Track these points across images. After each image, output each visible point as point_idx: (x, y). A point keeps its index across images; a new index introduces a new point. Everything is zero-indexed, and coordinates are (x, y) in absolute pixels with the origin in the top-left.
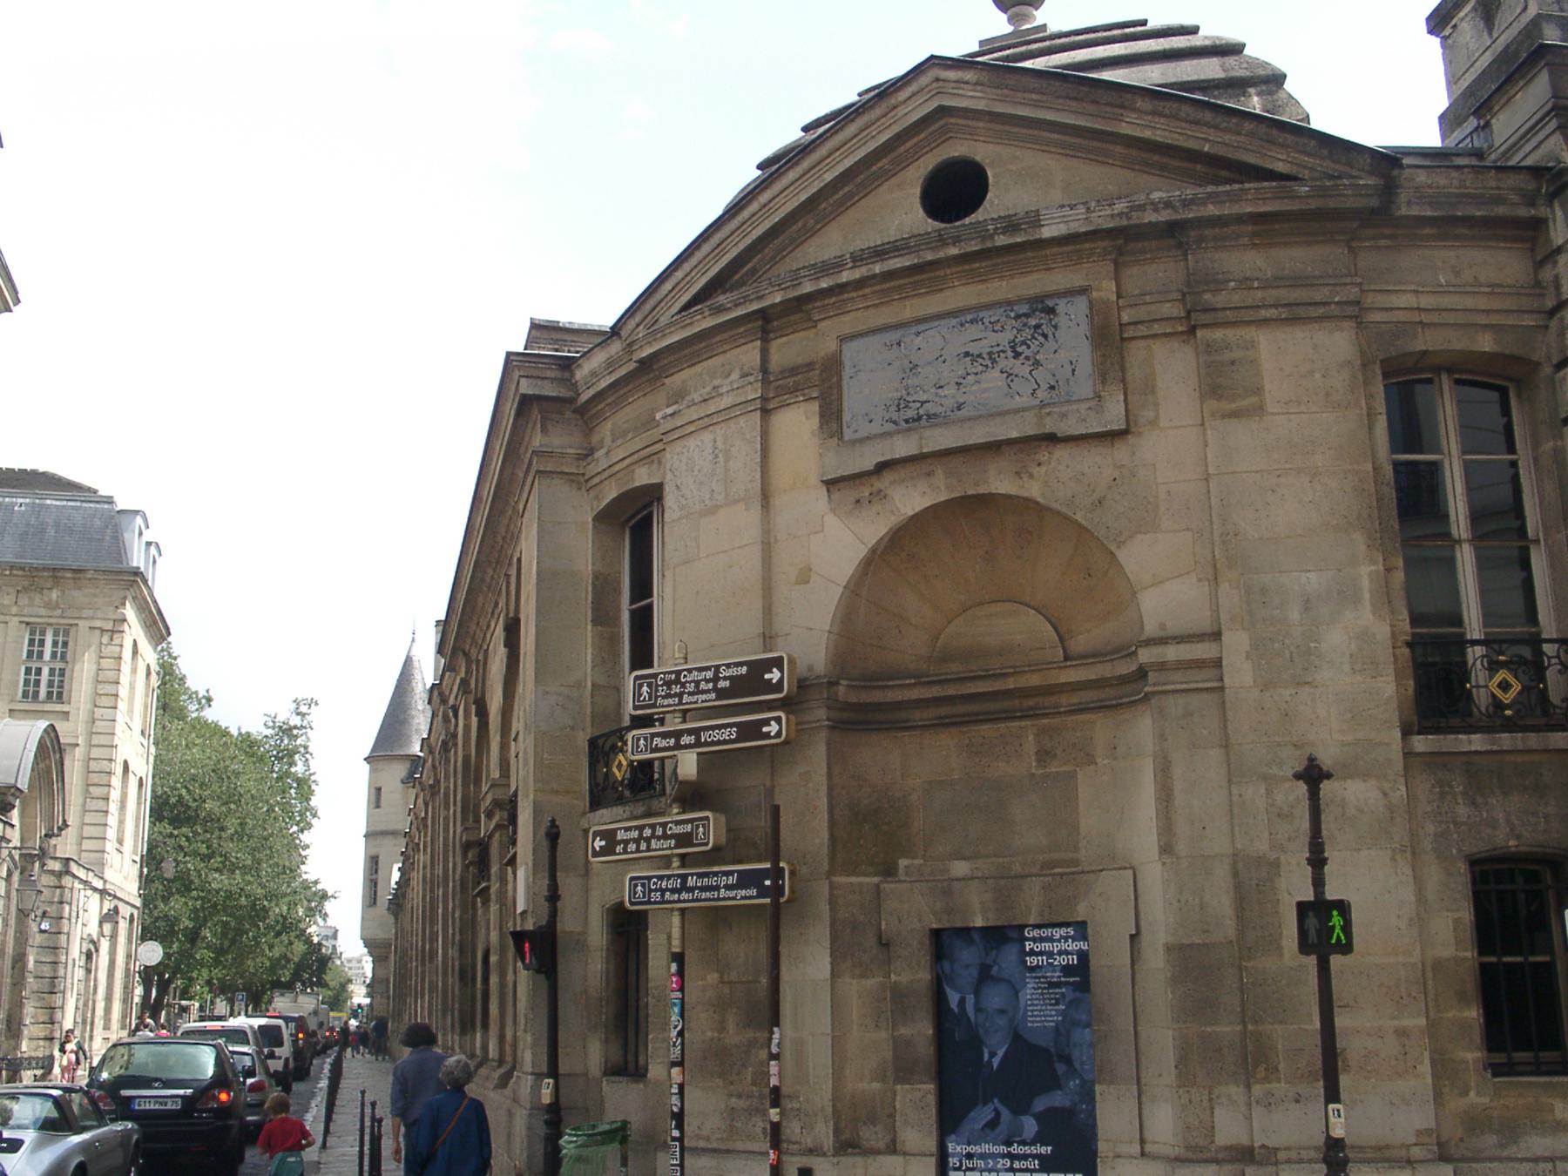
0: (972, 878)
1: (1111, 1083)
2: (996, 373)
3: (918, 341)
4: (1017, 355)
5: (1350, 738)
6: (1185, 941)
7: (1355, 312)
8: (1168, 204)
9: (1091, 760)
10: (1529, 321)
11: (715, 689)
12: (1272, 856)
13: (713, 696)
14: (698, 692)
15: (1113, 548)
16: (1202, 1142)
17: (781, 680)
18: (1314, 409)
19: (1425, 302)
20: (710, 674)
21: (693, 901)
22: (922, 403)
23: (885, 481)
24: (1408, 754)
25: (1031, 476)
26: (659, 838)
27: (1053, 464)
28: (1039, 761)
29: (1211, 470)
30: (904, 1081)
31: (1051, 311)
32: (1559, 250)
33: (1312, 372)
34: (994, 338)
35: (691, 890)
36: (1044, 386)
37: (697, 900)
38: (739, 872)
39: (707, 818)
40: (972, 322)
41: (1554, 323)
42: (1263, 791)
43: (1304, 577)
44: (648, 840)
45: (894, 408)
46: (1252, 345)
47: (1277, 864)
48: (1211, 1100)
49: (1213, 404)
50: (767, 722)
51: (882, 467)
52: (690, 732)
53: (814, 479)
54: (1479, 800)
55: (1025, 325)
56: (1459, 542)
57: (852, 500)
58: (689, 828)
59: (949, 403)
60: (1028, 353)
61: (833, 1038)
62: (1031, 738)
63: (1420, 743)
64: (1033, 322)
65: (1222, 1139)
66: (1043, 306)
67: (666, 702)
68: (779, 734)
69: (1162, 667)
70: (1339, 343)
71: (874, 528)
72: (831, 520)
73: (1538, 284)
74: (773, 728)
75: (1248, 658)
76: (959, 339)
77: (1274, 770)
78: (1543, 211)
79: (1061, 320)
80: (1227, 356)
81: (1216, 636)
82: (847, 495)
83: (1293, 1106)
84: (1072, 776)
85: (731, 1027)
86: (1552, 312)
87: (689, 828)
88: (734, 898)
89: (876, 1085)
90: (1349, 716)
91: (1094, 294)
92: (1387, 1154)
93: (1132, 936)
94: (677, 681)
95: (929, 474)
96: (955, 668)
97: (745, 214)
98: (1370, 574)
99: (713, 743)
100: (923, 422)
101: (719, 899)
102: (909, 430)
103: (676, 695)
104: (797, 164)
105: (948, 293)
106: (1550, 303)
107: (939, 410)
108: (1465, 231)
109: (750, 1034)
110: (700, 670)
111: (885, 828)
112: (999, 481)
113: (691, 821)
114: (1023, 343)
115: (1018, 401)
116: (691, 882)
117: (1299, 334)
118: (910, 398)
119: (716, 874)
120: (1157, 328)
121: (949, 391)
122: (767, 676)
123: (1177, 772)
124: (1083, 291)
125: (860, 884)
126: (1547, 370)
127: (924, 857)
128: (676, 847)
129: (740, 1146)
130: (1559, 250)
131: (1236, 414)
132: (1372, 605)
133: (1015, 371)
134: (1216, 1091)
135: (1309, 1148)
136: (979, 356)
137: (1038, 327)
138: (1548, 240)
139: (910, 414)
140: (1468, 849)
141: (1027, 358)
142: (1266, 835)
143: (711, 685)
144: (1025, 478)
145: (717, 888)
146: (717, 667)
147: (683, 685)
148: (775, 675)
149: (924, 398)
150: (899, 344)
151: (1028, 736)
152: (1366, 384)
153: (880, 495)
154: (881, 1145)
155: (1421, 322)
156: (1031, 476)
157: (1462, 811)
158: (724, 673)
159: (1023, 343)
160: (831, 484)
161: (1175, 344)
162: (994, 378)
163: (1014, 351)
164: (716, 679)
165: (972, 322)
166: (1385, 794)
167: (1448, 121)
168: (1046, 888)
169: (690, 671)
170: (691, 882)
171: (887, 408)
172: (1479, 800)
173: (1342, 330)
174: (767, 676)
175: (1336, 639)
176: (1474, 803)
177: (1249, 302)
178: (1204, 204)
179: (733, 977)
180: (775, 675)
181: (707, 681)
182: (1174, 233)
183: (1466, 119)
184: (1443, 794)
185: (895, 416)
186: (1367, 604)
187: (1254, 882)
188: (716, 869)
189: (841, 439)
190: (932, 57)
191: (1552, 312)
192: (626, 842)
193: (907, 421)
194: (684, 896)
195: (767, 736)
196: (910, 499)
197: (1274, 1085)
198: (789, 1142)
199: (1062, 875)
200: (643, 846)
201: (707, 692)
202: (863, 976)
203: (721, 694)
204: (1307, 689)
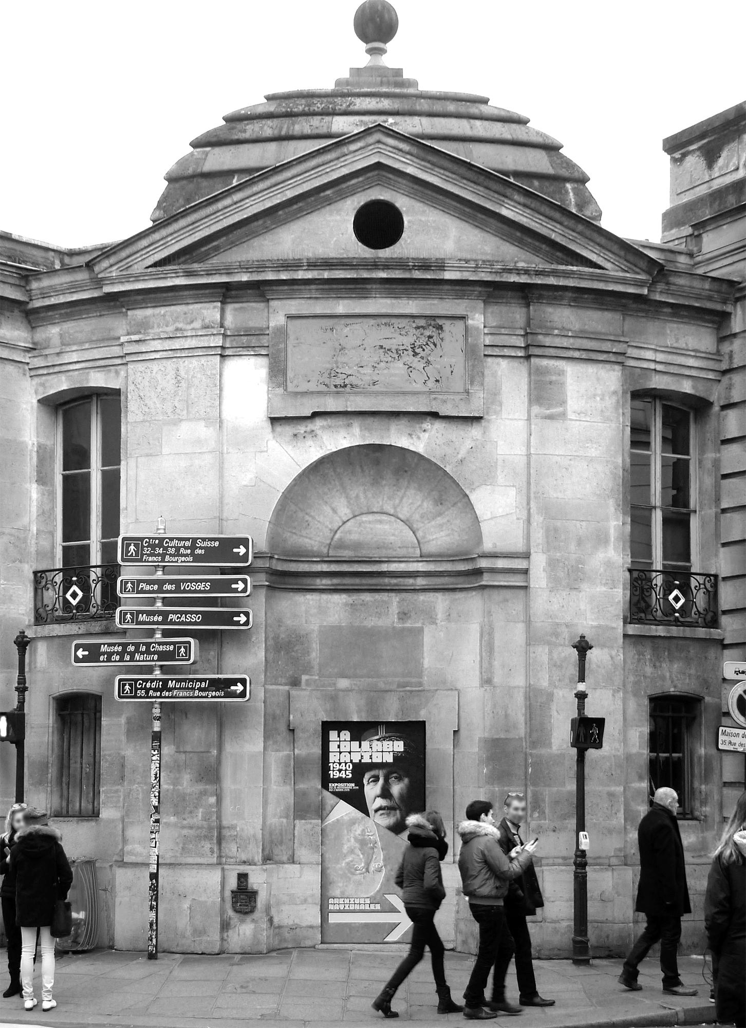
0: (351, 690)
2: (400, 364)
3: (346, 330)
4: (415, 354)
5: (595, 624)
7: (618, 359)
10: (711, 376)
11: (192, 554)
15: (467, 492)
20: (188, 544)
23: (319, 423)
24: (625, 636)
25: (419, 438)
26: (142, 653)
30: (302, 817)
31: (440, 328)
32: (735, 335)
36: (432, 379)
40: (386, 324)
41: (725, 380)
44: (132, 655)
45: (326, 375)
46: (562, 373)
49: (536, 409)
50: (236, 581)
51: (315, 415)
52: (171, 582)
54: (658, 664)
56: (655, 508)
57: (291, 434)
59: (367, 379)
60: (422, 354)
62: (395, 604)
63: (632, 629)
64: (427, 333)
66: (434, 321)
67: (150, 559)
68: (244, 590)
69: (493, 571)
70: (609, 379)
72: (273, 444)
73: (718, 352)
74: (241, 586)
76: (376, 335)
77: (554, 639)
78: (729, 308)
79: (446, 335)
80: (548, 378)
81: (527, 556)
82: (287, 430)
83: (552, 833)
84: (420, 631)
86: (724, 372)
87: (172, 648)
91: (470, 322)
92: (599, 861)
94: (160, 545)
96: (347, 554)
97: (220, 205)
99: (190, 591)
100: (348, 389)
102: (338, 393)
103: (159, 555)
104: (266, 178)
105: (370, 301)
106: (724, 366)
107: (360, 383)
108: (685, 313)
109: (200, 787)
110: (180, 539)
112: (398, 437)
113: (174, 643)
115: (419, 387)
116: (170, 684)
117: (591, 369)
119: (192, 680)
120: (506, 352)
121: (368, 370)
122: (235, 550)
123: (497, 636)
124: (463, 318)
126: (716, 408)
130: (735, 335)
131: (551, 417)
133: (414, 365)
137: (430, 337)
138: (729, 327)
139: (338, 382)
140: (649, 692)
141: (422, 358)
143: (189, 551)
144: (415, 439)
146: (194, 540)
147: (166, 549)
150: (332, 329)
151: (395, 599)
152: (623, 405)
154: (285, 858)
155: (655, 370)
156: (419, 438)
157: (649, 670)
158: (199, 544)
161: (515, 363)
162: (398, 367)
163: (414, 351)
164: (193, 547)
165: (386, 324)
166: (612, 658)
167: (671, 219)
168: (401, 699)
169: (171, 539)
170: (170, 684)
171: (322, 374)
172: (658, 664)
173: (614, 370)
174: (235, 550)
177: (565, 345)
178: (548, 276)
179: (188, 748)
180: (242, 550)
182: (526, 293)
183: (683, 224)
184: (639, 660)
185: (327, 381)
188: (191, 676)
191: (724, 372)
192: (110, 655)
193: (336, 386)
195: (236, 591)
198: (227, 857)
199: (411, 692)
200: (127, 658)
201: (186, 555)
204: (574, 592)
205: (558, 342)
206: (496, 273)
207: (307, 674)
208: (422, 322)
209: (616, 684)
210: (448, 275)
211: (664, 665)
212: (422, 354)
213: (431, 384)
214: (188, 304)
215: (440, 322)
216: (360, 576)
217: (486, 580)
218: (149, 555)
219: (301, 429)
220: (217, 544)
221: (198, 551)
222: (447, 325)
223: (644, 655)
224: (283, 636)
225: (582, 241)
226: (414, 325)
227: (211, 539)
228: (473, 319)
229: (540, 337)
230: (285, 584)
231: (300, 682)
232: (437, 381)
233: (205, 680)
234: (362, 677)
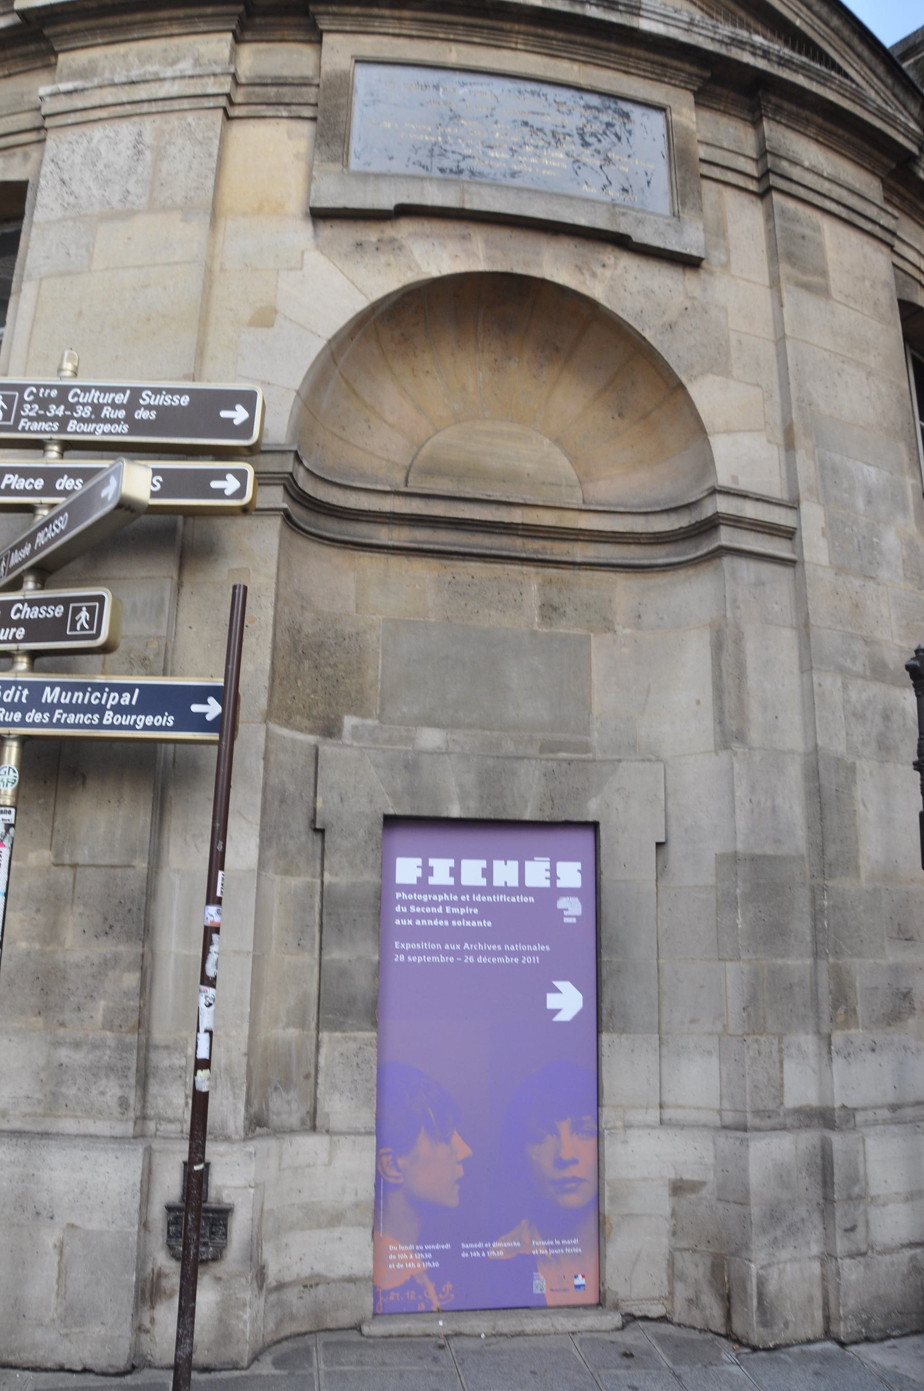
0: (447, 753)
1: (623, 1031)
3: (461, 92)
4: (586, 144)
6: (758, 851)
9: (608, 627)
11: (129, 419)
12: (849, 760)
13: (125, 428)
14: (97, 416)
15: (684, 380)
16: (771, 1105)
17: (249, 423)
20: (121, 398)
21: (50, 725)
22: (465, 157)
23: (404, 229)
25: (594, 275)
27: (619, 271)
28: (543, 617)
29: (788, 331)
30: (336, 1027)
33: (863, 278)
34: (559, 119)
35: (50, 708)
37: (59, 725)
38: (141, 687)
39: (101, 599)
42: (839, 684)
43: (866, 468)
47: (852, 769)
48: (781, 1050)
50: (221, 475)
51: (404, 211)
52: (74, 473)
53: (295, 205)
55: (596, 118)
58: (59, 611)
60: (597, 145)
61: (254, 957)
62: (534, 587)
65: (791, 1100)
68: (240, 493)
69: (737, 522)
71: (382, 279)
72: (314, 258)
74: (231, 485)
75: (824, 535)
77: (848, 664)
80: (799, 229)
81: (793, 505)
82: (343, 234)
83: (870, 1056)
84: (585, 642)
85: (71, 934)
87: (59, 611)
88: (132, 727)
89: (293, 1033)
90: (904, 622)
93: (659, 845)
94: (58, 401)
95: (464, 237)
98: (913, 486)
100: (465, 176)
101: (100, 726)
103: (55, 418)
107: (486, 170)
109: (106, 948)
111: (329, 671)
112: (554, 264)
113: (66, 601)
114: (593, 135)
116: (49, 696)
118: (447, 147)
119: (100, 687)
122: (224, 414)
125: (294, 741)
127: (379, 717)
128: (26, 639)
129: (69, 1125)
132: (916, 518)
133: (584, 159)
134: (787, 1039)
135: (881, 1107)
136: (541, 130)
137: (609, 125)
139: (447, 163)
142: (844, 733)
143: (122, 414)
144: (587, 275)
145: (100, 709)
146: (136, 393)
147: (71, 407)
148: (239, 415)
149: (468, 152)
150: (436, 87)
151: (532, 581)
153: (395, 246)
154: (294, 1121)
156: (594, 275)
158: (147, 399)
159: (593, 135)
160: (320, 216)
162: (556, 158)
163: (583, 139)
164: (133, 405)
165: (533, 93)
168: (549, 775)
169: (86, 389)
170: (49, 696)
174: (224, 414)
175: (891, 540)
177: (818, 188)
178: (796, 71)
179: (83, 856)
180: (239, 415)
181: (114, 406)
185: (426, 161)
186: (912, 514)
187: (834, 787)
189: (346, 164)
193: (442, 170)
194: (34, 716)
195: (220, 494)
196: (437, 256)
197: (853, 1031)
198: (160, 1118)
199: (570, 762)
201: (117, 421)
202: (287, 872)
203: (137, 427)
206: (721, 42)
207: (355, 714)
208: (595, 100)
210: (645, 25)
212: (597, 145)
213: (614, 193)
214: (171, 36)
215: (626, 107)
216: (465, 530)
217: (726, 537)
218: (31, 419)
219: (371, 233)
220: (185, 400)
221: (141, 414)
222: (637, 113)
225: (838, 43)
226: (582, 103)
227: (172, 392)
228: (679, 114)
231: (340, 730)
232: (625, 190)
233: (130, 688)
234: (470, 726)
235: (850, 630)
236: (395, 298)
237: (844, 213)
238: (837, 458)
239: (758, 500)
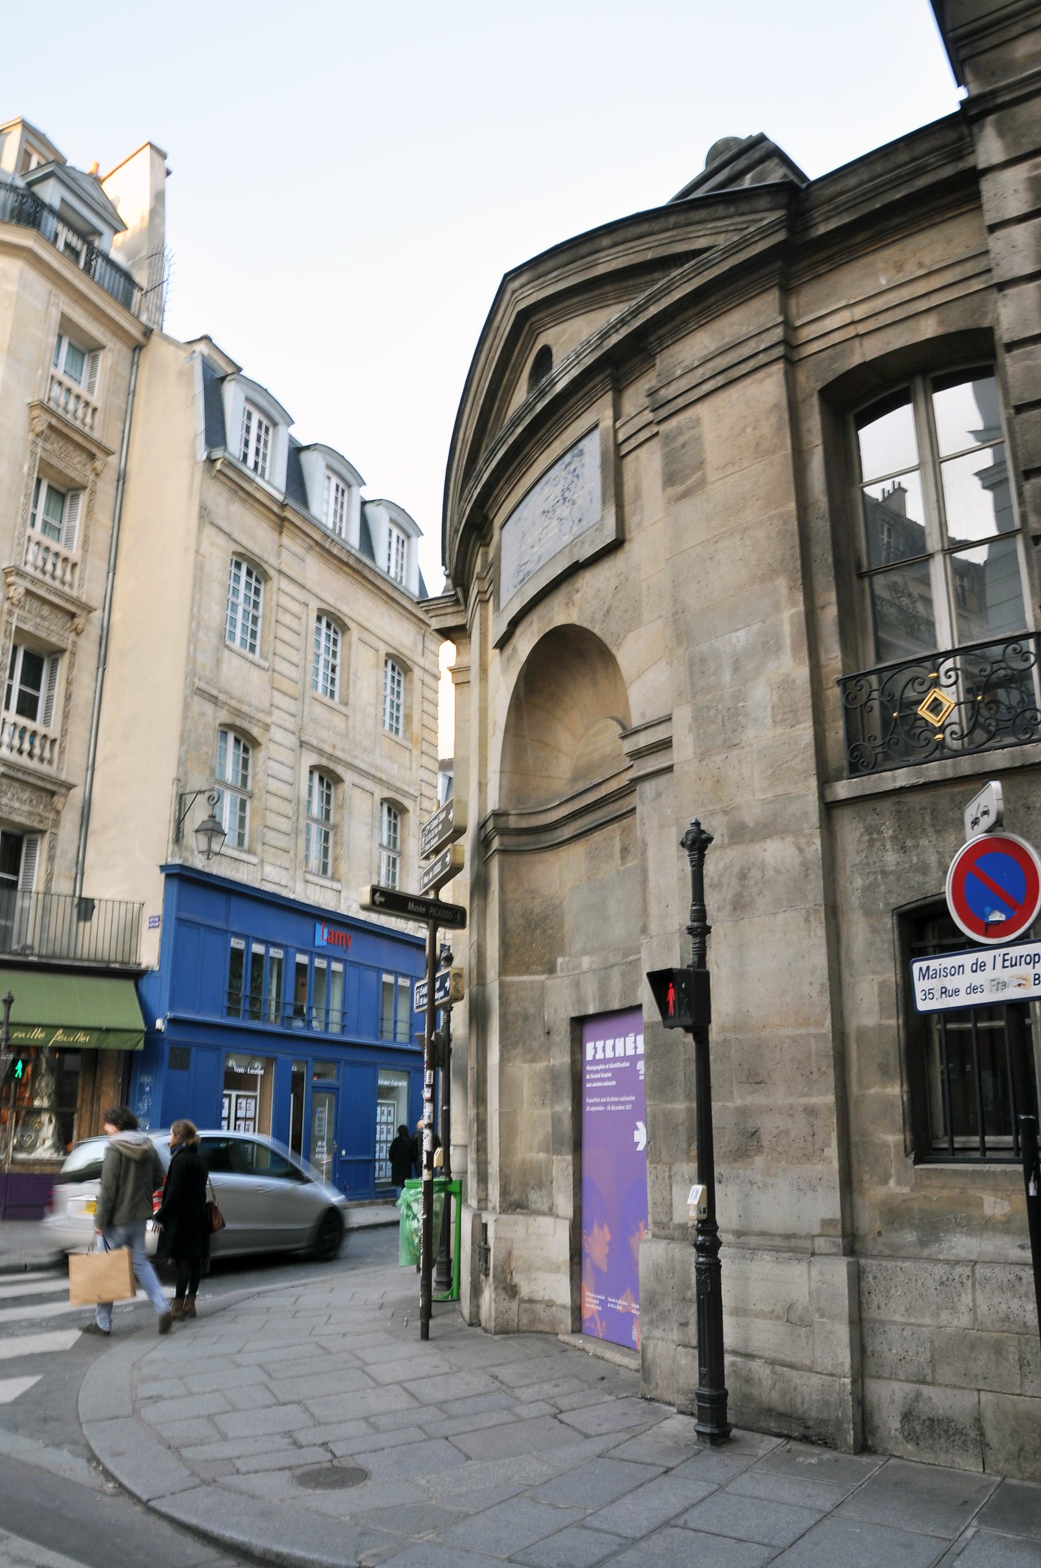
5: (769, 795)
8: (623, 322)
16: (665, 1220)
18: (745, 464)
19: (859, 312)
48: (670, 1177)
54: (909, 843)
75: (690, 730)
80: (681, 440)
90: (770, 772)
92: (793, 1243)
98: (792, 617)
108: (901, 220)
134: (675, 1169)
140: (896, 901)
154: (545, 1208)
155: (857, 336)
157: (891, 858)
166: (801, 850)
176: (904, 849)
184: (871, 842)
190: (506, 276)
202: (533, 1061)
204: (735, 752)
205: (683, 384)
209: (811, 897)
211: (924, 842)
223: (880, 833)
224: (537, 910)
229: (663, 392)
230: (535, 844)
235: (711, 808)
236: (522, 685)
237: (720, 380)
238: (704, 647)
239: (646, 728)
